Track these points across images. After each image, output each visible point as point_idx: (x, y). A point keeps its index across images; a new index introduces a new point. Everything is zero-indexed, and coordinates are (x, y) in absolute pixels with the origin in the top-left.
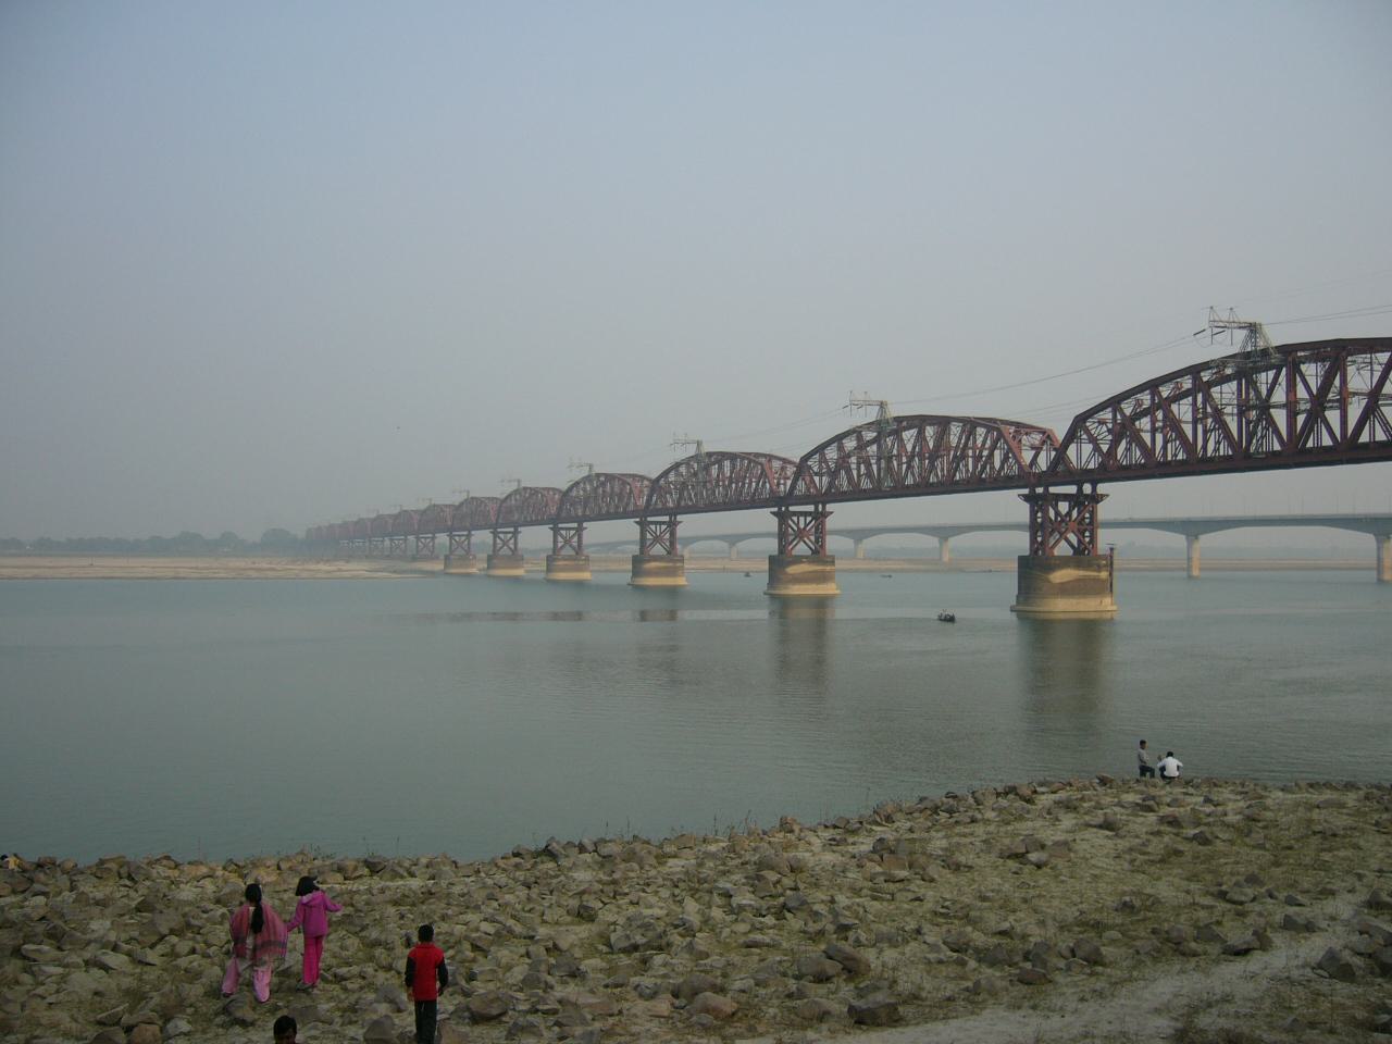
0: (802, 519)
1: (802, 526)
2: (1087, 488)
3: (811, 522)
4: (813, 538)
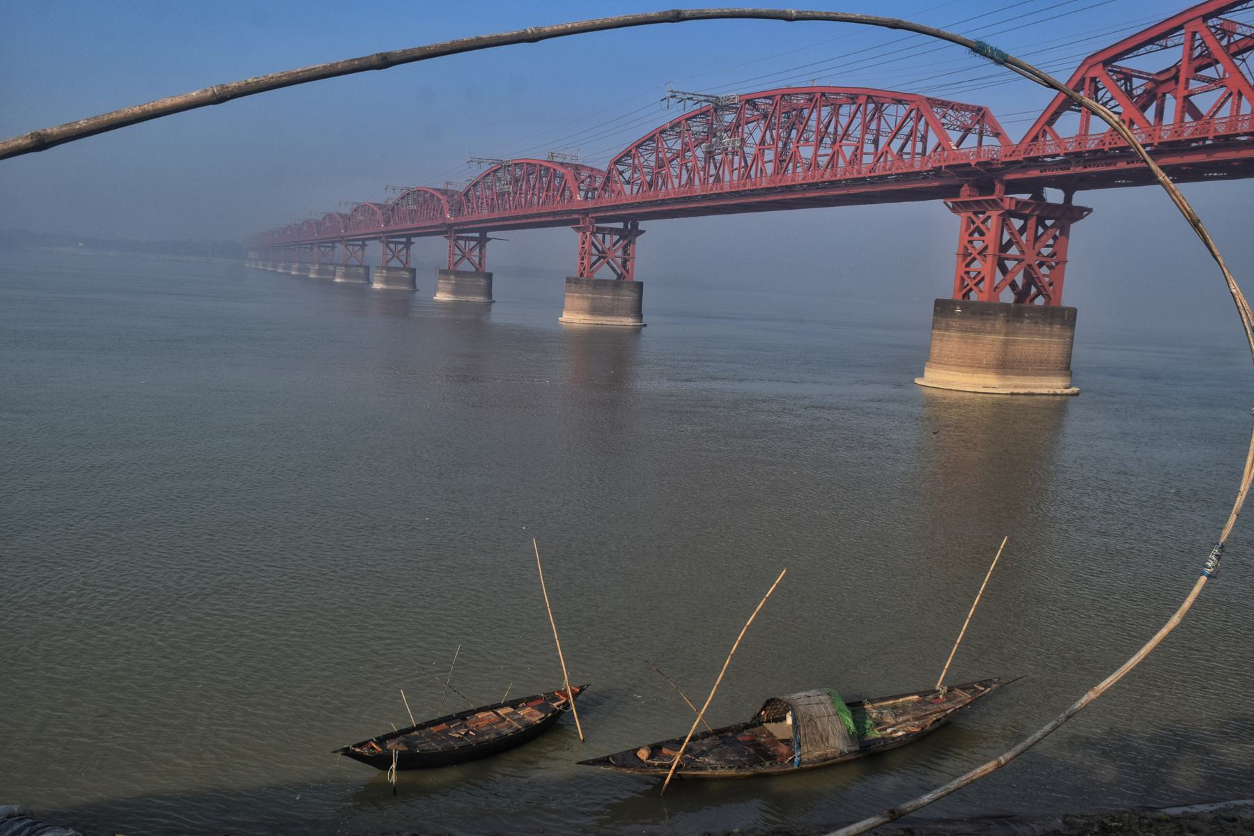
0: (608, 237)
1: (608, 244)
2: (1054, 196)
3: (617, 241)
4: (619, 261)
